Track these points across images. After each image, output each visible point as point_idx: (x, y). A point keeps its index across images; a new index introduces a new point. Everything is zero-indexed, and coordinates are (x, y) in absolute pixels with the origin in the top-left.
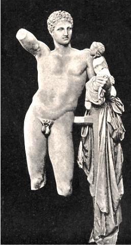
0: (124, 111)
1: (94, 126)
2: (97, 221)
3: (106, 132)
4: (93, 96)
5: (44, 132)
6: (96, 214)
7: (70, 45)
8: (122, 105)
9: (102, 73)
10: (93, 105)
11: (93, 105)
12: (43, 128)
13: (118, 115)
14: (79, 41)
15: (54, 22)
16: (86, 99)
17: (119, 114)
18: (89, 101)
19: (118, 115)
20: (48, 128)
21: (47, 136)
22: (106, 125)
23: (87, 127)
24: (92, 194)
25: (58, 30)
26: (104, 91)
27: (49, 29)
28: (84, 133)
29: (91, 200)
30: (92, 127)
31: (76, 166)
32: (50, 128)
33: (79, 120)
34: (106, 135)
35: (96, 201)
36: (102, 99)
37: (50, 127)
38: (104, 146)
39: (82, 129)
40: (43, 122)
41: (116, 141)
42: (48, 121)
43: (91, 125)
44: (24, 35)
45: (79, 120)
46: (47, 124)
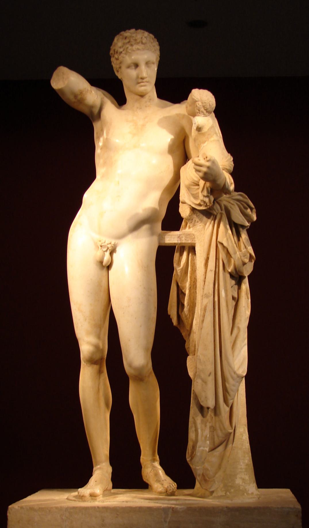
0: (255, 218)
1: (197, 249)
2: (195, 423)
3: (217, 259)
5: (101, 262)
6: (193, 410)
8: (251, 209)
9: (213, 150)
10: (193, 210)
12: (99, 253)
13: (241, 229)
14: (172, 88)
15: (121, 52)
16: (181, 198)
17: (243, 227)
18: (183, 203)
19: (241, 229)
20: (107, 254)
21: (109, 267)
23: (185, 254)
24: (191, 374)
25: (129, 67)
26: (208, 184)
27: (114, 66)
28: (181, 261)
29: (188, 382)
30: (195, 254)
32: (111, 254)
33: (172, 238)
35: (197, 387)
36: (207, 200)
37: (111, 254)
38: (212, 286)
39: (176, 255)
40: (99, 244)
41: (237, 277)
42: (107, 242)
43: (192, 249)
45: (172, 238)
46: (105, 246)
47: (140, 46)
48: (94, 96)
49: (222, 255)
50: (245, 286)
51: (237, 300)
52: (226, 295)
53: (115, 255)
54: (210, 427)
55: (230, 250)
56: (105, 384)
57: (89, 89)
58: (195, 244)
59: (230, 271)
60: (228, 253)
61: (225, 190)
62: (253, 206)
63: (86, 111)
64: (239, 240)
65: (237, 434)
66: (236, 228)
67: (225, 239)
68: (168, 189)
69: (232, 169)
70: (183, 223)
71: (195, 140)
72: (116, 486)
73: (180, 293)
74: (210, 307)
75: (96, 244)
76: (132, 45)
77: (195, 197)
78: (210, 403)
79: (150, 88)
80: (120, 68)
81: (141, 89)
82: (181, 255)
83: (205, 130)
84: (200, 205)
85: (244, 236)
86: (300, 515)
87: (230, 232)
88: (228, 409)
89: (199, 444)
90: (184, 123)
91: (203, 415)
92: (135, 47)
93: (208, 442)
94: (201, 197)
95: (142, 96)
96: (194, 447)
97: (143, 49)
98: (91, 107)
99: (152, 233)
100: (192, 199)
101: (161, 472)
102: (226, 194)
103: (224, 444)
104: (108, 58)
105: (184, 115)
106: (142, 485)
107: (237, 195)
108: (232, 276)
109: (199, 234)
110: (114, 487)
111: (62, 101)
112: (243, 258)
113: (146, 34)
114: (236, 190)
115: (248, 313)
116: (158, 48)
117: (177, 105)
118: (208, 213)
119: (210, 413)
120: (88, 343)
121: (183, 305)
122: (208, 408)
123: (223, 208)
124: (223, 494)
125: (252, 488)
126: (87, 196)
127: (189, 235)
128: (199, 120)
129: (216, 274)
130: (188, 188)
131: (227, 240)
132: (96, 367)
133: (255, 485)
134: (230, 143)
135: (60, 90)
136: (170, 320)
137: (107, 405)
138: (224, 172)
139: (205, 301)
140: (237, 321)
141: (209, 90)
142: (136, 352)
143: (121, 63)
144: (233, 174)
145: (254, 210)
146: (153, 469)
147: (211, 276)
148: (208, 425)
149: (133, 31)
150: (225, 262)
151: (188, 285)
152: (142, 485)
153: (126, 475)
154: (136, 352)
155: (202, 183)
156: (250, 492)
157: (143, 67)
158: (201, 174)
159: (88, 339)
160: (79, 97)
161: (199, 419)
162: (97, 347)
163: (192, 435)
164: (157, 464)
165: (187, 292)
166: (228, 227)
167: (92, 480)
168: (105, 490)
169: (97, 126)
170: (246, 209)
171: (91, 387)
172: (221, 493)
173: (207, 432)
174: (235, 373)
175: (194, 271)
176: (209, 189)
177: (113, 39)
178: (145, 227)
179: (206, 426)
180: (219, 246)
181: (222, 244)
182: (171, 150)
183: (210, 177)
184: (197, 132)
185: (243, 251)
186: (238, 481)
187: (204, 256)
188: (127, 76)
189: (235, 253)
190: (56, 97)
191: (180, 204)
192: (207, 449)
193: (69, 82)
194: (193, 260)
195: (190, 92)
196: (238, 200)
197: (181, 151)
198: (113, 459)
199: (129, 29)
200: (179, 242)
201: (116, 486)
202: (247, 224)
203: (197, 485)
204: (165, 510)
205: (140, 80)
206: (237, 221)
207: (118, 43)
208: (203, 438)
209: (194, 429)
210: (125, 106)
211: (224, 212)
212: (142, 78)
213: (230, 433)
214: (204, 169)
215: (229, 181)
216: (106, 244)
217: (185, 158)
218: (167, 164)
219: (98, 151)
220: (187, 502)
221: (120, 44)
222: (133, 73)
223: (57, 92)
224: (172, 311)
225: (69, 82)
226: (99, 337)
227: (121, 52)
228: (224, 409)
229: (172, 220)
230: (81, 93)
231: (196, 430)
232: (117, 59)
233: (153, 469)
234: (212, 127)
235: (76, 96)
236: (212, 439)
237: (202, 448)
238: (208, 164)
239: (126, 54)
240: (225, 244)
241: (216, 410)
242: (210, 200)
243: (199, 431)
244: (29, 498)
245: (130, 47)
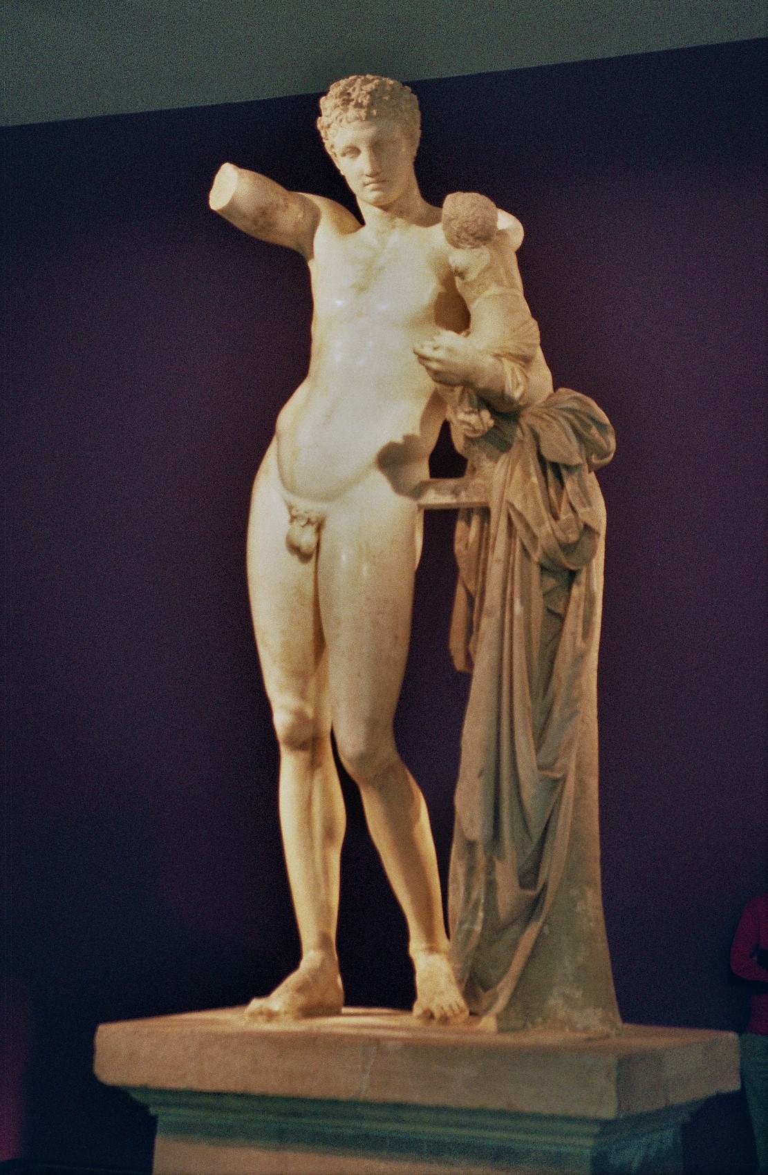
2: (455, 875)
10: (467, 439)
13: (564, 472)
17: (568, 467)
34: (509, 551)
36: (473, 419)
40: (294, 513)
44: (231, 187)
46: (302, 517)
53: (326, 534)
55: (530, 518)
56: (326, 793)
57: (281, 202)
58: (487, 503)
60: (528, 527)
62: (606, 421)
63: (289, 243)
66: (554, 471)
67: (520, 496)
87: (535, 480)
99: (399, 487)
110: (349, 1002)
112: (559, 534)
123: (526, 430)
131: (525, 497)
132: (304, 756)
136: (451, 659)
145: (611, 428)
150: (525, 542)
156: (579, 1026)
160: (261, 221)
166: (533, 467)
170: (589, 427)
176: (475, 398)
181: (512, 505)
189: (541, 523)
192: (478, 928)
196: (572, 411)
200: (454, 501)
206: (549, 456)
208: (471, 906)
211: (528, 439)
216: (301, 512)
229: (447, 462)
237: (466, 926)
240: (518, 506)
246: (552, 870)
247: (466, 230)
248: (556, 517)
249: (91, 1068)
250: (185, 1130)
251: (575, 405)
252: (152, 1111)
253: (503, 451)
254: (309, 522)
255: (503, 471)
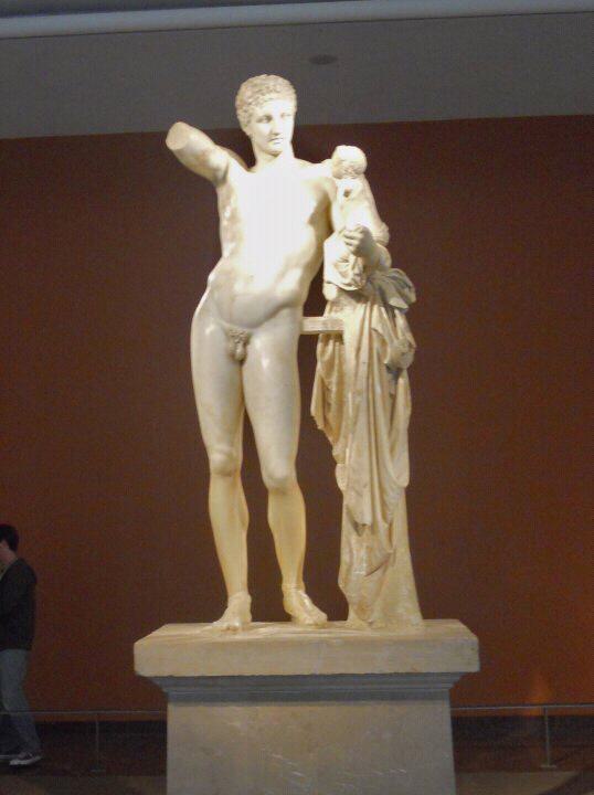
0: (413, 298)
1: (347, 337)
2: (349, 543)
3: (371, 349)
4: (338, 276)
7: (288, 150)
10: (341, 290)
11: (341, 290)
12: (231, 345)
13: (397, 312)
14: (311, 145)
15: (250, 104)
18: (329, 283)
21: (242, 362)
22: (370, 335)
23: (331, 342)
24: (342, 485)
25: (260, 121)
26: (360, 261)
28: (324, 352)
29: (339, 496)
31: (307, 422)
33: (314, 325)
36: (358, 279)
38: (364, 380)
39: (320, 346)
41: (394, 371)
43: (339, 337)
45: (314, 325)
47: (273, 95)
48: (221, 158)
49: (376, 345)
50: (403, 381)
51: (393, 397)
52: (383, 392)
53: (249, 347)
54: (367, 547)
55: (386, 338)
59: (386, 362)
61: (378, 265)
62: (410, 284)
64: (395, 326)
65: (398, 555)
68: (308, 267)
69: (386, 241)
70: (328, 308)
71: (342, 208)
72: (255, 619)
73: (325, 390)
74: (363, 406)
75: (226, 334)
76: (263, 94)
77: (344, 275)
78: (368, 520)
79: (285, 145)
80: (249, 122)
81: (272, 146)
82: (326, 344)
83: (352, 196)
84: (349, 285)
85: (401, 321)
86: (477, 648)
88: (386, 526)
89: (355, 566)
90: (327, 187)
91: (359, 535)
92: (267, 96)
93: (365, 565)
94: (351, 274)
95: (275, 155)
96: (349, 570)
97: (278, 98)
98: (216, 170)
100: (339, 276)
101: (307, 601)
102: (380, 270)
103: (383, 568)
104: (233, 110)
105: (327, 178)
106: (284, 617)
107: (393, 272)
108: (388, 368)
109: (350, 319)
111: (180, 164)
113: (280, 80)
114: (393, 266)
115: (409, 412)
116: (294, 96)
117: (317, 166)
118: (358, 296)
119: (367, 531)
120: (221, 452)
121: (329, 405)
122: (364, 525)
124: (384, 625)
125: (415, 616)
126: (212, 277)
127: (337, 322)
128: (343, 184)
129: (370, 365)
130: (336, 266)
133: (419, 614)
134: (384, 209)
135: (179, 151)
136: (314, 422)
137: (243, 524)
138: (379, 245)
139: (358, 399)
140: (395, 422)
141: (359, 146)
142: (278, 462)
143: (251, 115)
144: (389, 247)
145: (413, 290)
146: (296, 597)
147: (363, 369)
148: (365, 544)
149: (263, 76)
151: (334, 379)
152: (284, 617)
153: (268, 606)
154: (278, 462)
155: (352, 258)
157: (276, 118)
158: (352, 248)
159: (220, 449)
161: (354, 538)
162: (229, 455)
163: (345, 557)
164: (302, 593)
165: (334, 388)
167: (228, 613)
168: (243, 623)
169: (222, 192)
170: (403, 288)
171: (225, 508)
172: (380, 625)
173: (363, 553)
174: (395, 483)
175: (341, 364)
177: (239, 88)
178: (285, 312)
179: (362, 546)
180: (373, 332)
181: (376, 331)
182: (312, 221)
183: (363, 249)
184: (344, 198)
185: (401, 337)
186: (400, 610)
187: (355, 344)
188: (257, 131)
189: (392, 341)
190: (171, 159)
191: (325, 285)
192: (364, 573)
193: (187, 140)
194: (340, 350)
195: (333, 150)
196: (394, 278)
197: (324, 222)
198: (253, 586)
199: (259, 74)
201: (255, 619)
202: (405, 306)
203: (352, 614)
204: (320, 643)
205: (274, 136)
207: (246, 91)
209: (347, 550)
210: (255, 168)
211: (377, 293)
212: (277, 134)
213: (389, 554)
214: (356, 242)
215: (385, 256)
217: (330, 230)
218: (306, 237)
219: (224, 223)
220: (343, 635)
221: (249, 93)
222: (264, 128)
223: (177, 155)
224: (314, 409)
225: (187, 140)
226: (232, 444)
227: (250, 104)
228: (383, 526)
230: (204, 153)
231: (351, 551)
232: (246, 111)
233: (296, 597)
234: (363, 191)
235: (197, 157)
236: (370, 563)
238: (360, 236)
239: (256, 105)
240: (380, 331)
241: (373, 528)
242: (362, 279)
243: (355, 552)
244: (156, 633)
245: (261, 97)
246: (395, 538)
247: (352, 167)
248: (398, 338)
249: (133, 667)
250: (187, 700)
251: (394, 274)
252: (165, 690)
253: (358, 301)
254: (241, 339)
255: (362, 311)
